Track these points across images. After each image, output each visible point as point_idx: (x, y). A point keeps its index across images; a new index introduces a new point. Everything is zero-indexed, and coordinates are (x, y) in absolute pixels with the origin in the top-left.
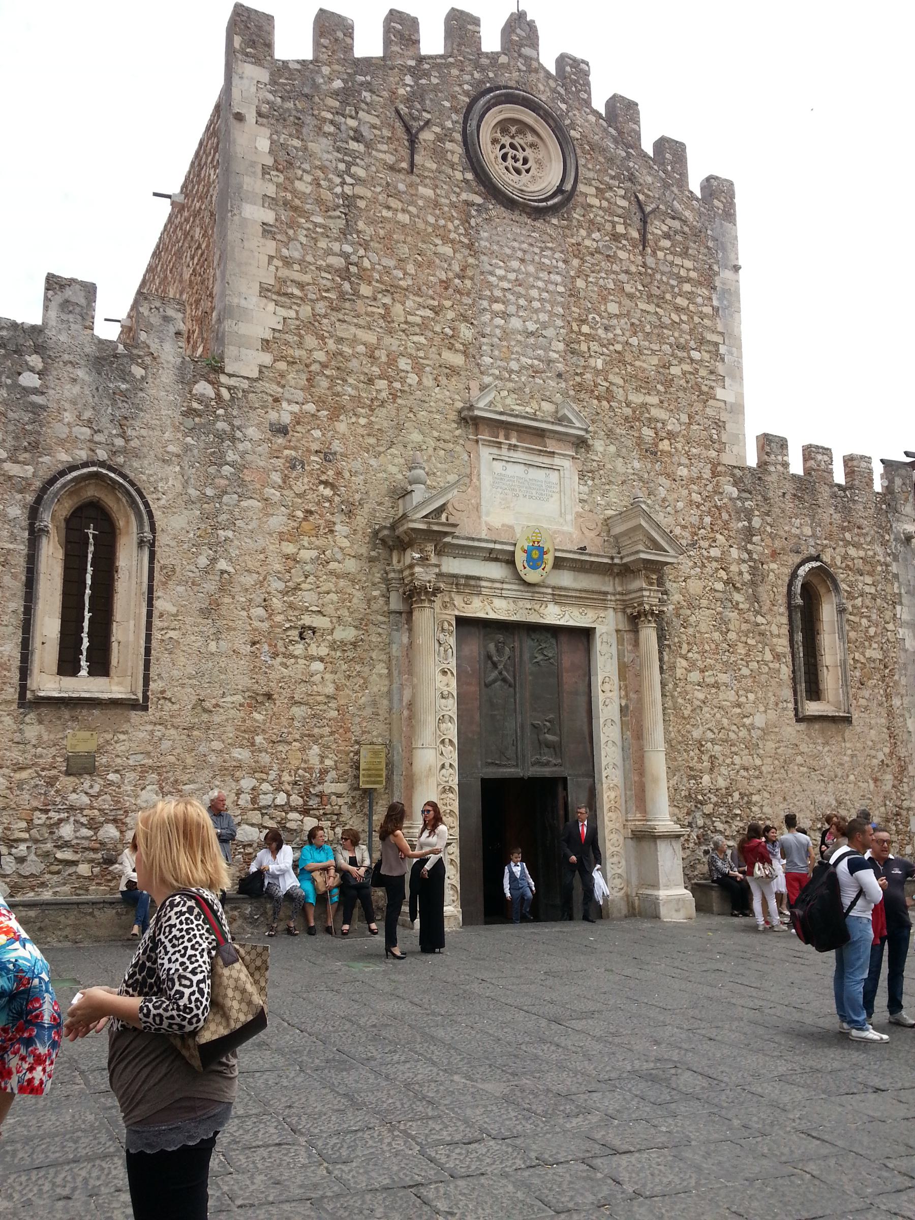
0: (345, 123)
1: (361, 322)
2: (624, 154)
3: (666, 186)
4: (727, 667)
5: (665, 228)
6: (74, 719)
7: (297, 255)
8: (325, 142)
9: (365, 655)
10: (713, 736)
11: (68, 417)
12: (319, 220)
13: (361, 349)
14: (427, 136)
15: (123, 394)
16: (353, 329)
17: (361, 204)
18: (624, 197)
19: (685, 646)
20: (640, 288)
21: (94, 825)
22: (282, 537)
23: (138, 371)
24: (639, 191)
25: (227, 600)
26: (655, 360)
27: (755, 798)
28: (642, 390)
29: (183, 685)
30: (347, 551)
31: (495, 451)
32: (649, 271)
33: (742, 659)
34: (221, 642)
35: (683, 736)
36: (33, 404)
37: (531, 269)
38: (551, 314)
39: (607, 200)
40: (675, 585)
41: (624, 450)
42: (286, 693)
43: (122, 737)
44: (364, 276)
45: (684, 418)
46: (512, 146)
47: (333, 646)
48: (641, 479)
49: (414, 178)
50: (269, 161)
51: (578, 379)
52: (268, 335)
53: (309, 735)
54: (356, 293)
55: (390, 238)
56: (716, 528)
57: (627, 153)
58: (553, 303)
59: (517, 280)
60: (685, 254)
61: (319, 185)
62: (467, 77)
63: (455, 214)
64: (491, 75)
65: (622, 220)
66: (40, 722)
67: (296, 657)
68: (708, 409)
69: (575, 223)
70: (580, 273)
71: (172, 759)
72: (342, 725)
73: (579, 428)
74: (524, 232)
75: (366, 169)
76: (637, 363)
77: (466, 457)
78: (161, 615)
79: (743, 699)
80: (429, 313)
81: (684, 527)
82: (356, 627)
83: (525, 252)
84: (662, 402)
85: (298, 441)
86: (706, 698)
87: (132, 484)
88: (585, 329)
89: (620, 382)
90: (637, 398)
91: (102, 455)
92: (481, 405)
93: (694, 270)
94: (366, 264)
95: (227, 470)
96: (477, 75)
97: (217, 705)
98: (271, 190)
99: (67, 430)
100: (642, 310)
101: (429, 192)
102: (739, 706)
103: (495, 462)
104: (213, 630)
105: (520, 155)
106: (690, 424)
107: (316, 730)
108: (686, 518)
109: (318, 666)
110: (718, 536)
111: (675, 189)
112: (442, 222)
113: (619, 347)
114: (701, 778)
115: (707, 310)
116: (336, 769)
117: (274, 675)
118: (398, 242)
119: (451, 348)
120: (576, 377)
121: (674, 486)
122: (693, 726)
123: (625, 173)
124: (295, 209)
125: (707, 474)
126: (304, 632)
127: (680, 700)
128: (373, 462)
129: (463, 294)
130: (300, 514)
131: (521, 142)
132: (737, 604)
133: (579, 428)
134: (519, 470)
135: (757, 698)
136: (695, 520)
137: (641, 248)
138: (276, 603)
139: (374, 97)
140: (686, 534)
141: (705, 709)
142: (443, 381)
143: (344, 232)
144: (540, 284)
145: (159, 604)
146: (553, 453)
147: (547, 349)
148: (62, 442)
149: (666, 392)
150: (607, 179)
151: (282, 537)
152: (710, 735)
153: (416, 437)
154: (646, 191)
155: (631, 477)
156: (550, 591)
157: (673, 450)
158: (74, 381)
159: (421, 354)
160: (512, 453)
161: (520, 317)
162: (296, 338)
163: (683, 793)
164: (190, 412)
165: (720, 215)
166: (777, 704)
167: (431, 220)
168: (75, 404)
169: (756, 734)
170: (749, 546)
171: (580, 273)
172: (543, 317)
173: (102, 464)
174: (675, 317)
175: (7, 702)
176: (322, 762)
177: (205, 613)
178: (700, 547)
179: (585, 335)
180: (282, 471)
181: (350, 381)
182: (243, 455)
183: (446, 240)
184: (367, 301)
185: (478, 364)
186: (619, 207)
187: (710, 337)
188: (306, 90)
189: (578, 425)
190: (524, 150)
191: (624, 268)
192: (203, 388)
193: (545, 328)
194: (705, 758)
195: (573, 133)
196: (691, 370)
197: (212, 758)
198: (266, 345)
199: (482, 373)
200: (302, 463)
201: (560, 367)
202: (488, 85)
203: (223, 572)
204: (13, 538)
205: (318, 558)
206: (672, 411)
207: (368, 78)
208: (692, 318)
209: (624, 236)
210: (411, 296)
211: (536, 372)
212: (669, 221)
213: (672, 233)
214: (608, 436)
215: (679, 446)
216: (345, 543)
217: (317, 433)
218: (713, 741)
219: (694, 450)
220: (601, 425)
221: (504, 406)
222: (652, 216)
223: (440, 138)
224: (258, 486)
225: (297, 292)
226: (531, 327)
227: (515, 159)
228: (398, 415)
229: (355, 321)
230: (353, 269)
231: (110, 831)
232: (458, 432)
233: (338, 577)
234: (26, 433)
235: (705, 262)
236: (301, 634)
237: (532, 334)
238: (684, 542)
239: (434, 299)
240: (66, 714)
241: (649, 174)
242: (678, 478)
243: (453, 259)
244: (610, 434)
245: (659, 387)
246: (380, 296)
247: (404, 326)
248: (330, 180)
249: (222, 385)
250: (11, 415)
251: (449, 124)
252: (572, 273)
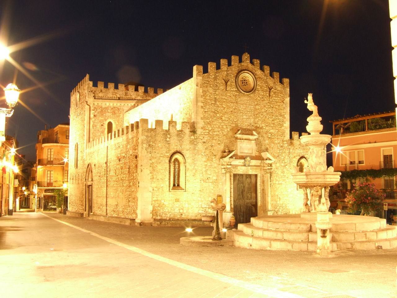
2: (266, 78)
3: (275, 83)
7: (206, 110)
8: (211, 88)
14: (229, 83)
21: (179, 210)
25: (196, 173)
31: (240, 142)
36: (168, 143)
52: (202, 126)
94: (218, 110)
95: (196, 151)
96: (238, 69)
105: (245, 82)
111: (276, 83)
115: (282, 108)
127: (274, 187)
128: (220, 147)
151: (205, 162)
170: (290, 156)
175: (168, 191)
182: (198, 148)
183: (231, 102)
192: (193, 137)
198: (202, 128)
202: (240, 70)
204: (167, 166)
227: (245, 83)
230: (216, 112)
231: (181, 211)
249: (195, 136)
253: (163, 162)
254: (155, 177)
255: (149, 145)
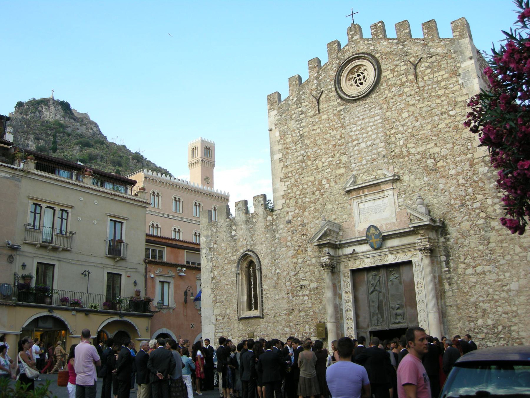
0: (298, 111)
1: (309, 174)
2: (402, 47)
4: (489, 262)
5: (427, 64)
6: (249, 323)
7: (289, 163)
9: (320, 291)
10: (483, 299)
11: (241, 240)
12: (294, 148)
13: (310, 184)
14: (324, 96)
15: (252, 228)
16: (307, 178)
17: (305, 134)
18: (404, 65)
19: (462, 258)
20: (418, 98)
22: (293, 257)
23: (254, 220)
24: (411, 57)
25: (280, 282)
26: (430, 126)
27: (513, 328)
28: (424, 144)
29: (271, 310)
30: (311, 256)
31: (359, 200)
32: (422, 88)
33: (500, 256)
34: (279, 295)
35: (465, 302)
37: (367, 120)
38: (377, 133)
39: (396, 71)
40: (453, 228)
41: (418, 175)
42: (297, 308)
43: (259, 327)
44: (309, 158)
45: (450, 146)
46: (359, 75)
47: (310, 290)
48: (429, 185)
49: (321, 114)
50: (279, 138)
51: (393, 154)
52: (283, 193)
53: (305, 322)
54: (307, 165)
55: (315, 140)
56: (475, 193)
57: (403, 45)
58: (377, 129)
59: (361, 128)
60: (440, 69)
61: (293, 136)
62: (334, 66)
63: (335, 118)
64: (342, 58)
65: (404, 75)
66: (242, 324)
67: (300, 296)
68: (463, 135)
69: (382, 90)
70: (388, 109)
71: (270, 332)
72: (314, 317)
73: (391, 176)
74: (362, 108)
75: (306, 122)
76: (420, 133)
77: (349, 207)
78: (265, 290)
79: (502, 277)
80: (331, 159)
81: (456, 199)
82: (317, 282)
83: (363, 115)
84: (436, 144)
85: (294, 223)
86: (477, 280)
87: (255, 253)
88: (393, 131)
89: (413, 145)
90: (421, 149)
91: (249, 248)
92: (348, 185)
93: (446, 73)
94: (309, 154)
95: (277, 240)
96: (337, 62)
97: (280, 315)
98: (280, 147)
99: (241, 243)
100: (420, 108)
101: (325, 116)
102: (499, 280)
103: (360, 204)
104: (277, 292)
105: (362, 77)
106: (453, 147)
107: (307, 320)
108: (456, 194)
109: (306, 298)
110: (478, 196)
112: (332, 123)
113: (410, 131)
114: (477, 321)
116: (314, 332)
117: (294, 303)
118: (318, 140)
119: (340, 167)
120: (392, 154)
121: (447, 181)
122: (470, 296)
123: (403, 54)
124: (287, 148)
125: (467, 166)
126: (302, 287)
128: (317, 222)
129: (341, 145)
130: (297, 248)
131: (361, 71)
132: (494, 227)
133: (391, 176)
134: (370, 204)
135: (511, 275)
136: (463, 193)
137: (415, 81)
138: (293, 279)
139: (306, 95)
140: (458, 202)
141: (477, 286)
142: (338, 181)
143: (301, 147)
144: (371, 124)
145: (265, 287)
146: (384, 191)
147: (376, 149)
148: (241, 247)
149: (438, 138)
150: (396, 63)
152: (481, 299)
153: (330, 207)
154: (415, 55)
155: (424, 185)
156: (387, 250)
157: (445, 164)
158: (242, 229)
159: (329, 175)
160: (366, 198)
161: (364, 142)
162: (291, 190)
163: (466, 330)
164: (267, 227)
165: (457, 38)
166: (526, 275)
167: (327, 125)
168: (242, 236)
169: (511, 294)
171: (388, 109)
172: (374, 136)
173: (249, 250)
174: (438, 101)
175: (236, 320)
176: (310, 330)
177: (274, 287)
178: (467, 206)
179: (394, 134)
180: (291, 236)
181: (308, 196)
184: (311, 166)
185: (350, 169)
186: (402, 70)
187: (459, 99)
188: (286, 109)
189: (390, 175)
190: (362, 73)
191: (408, 95)
192: (269, 218)
193: (375, 140)
194: (479, 311)
195: (377, 55)
196: (451, 121)
197: (280, 331)
199: (352, 171)
200: (296, 231)
201: (384, 153)
202: (342, 62)
203: (278, 273)
204: (234, 277)
205: (303, 261)
206: (442, 146)
207: (303, 91)
208: (448, 96)
209: (406, 81)
210: (323, 156)
211: (374, 160)
212: (430, 60)
213: (431, 65)
214: (410, 172)
215: (448, 161)
216: (310, 253)
217: (299, 219)
218: (483, 302)
219: (458, 159)
220: (406, 168)
221: (362, 180)
222: (419, 64)
223: (327, 94)
224: (285, 243)
225: (290, 175)
226: (369, 143)
227: (360, 79)
228: (323, 202)
229: (307, 175)
232: (345, 199)
233: (309, 266)
234: (234, 247)
235: (451, 66)
236: (301, 288)
237: (370, 146)
238: (456, 206)
239: (331, 153)
240: (247, 321)
241: (415, 46)
242: (449, 176)
243: (336, 135)
244: (410, 171)
245: (433, 138)
246: (314, 162)
247: (323, 168)
248: (295, 133)
250: (231, 244)
251: (330, 87)
252: (384, 112)
253: (229, 271)
254: (218, 297)
255: (210, 249)
